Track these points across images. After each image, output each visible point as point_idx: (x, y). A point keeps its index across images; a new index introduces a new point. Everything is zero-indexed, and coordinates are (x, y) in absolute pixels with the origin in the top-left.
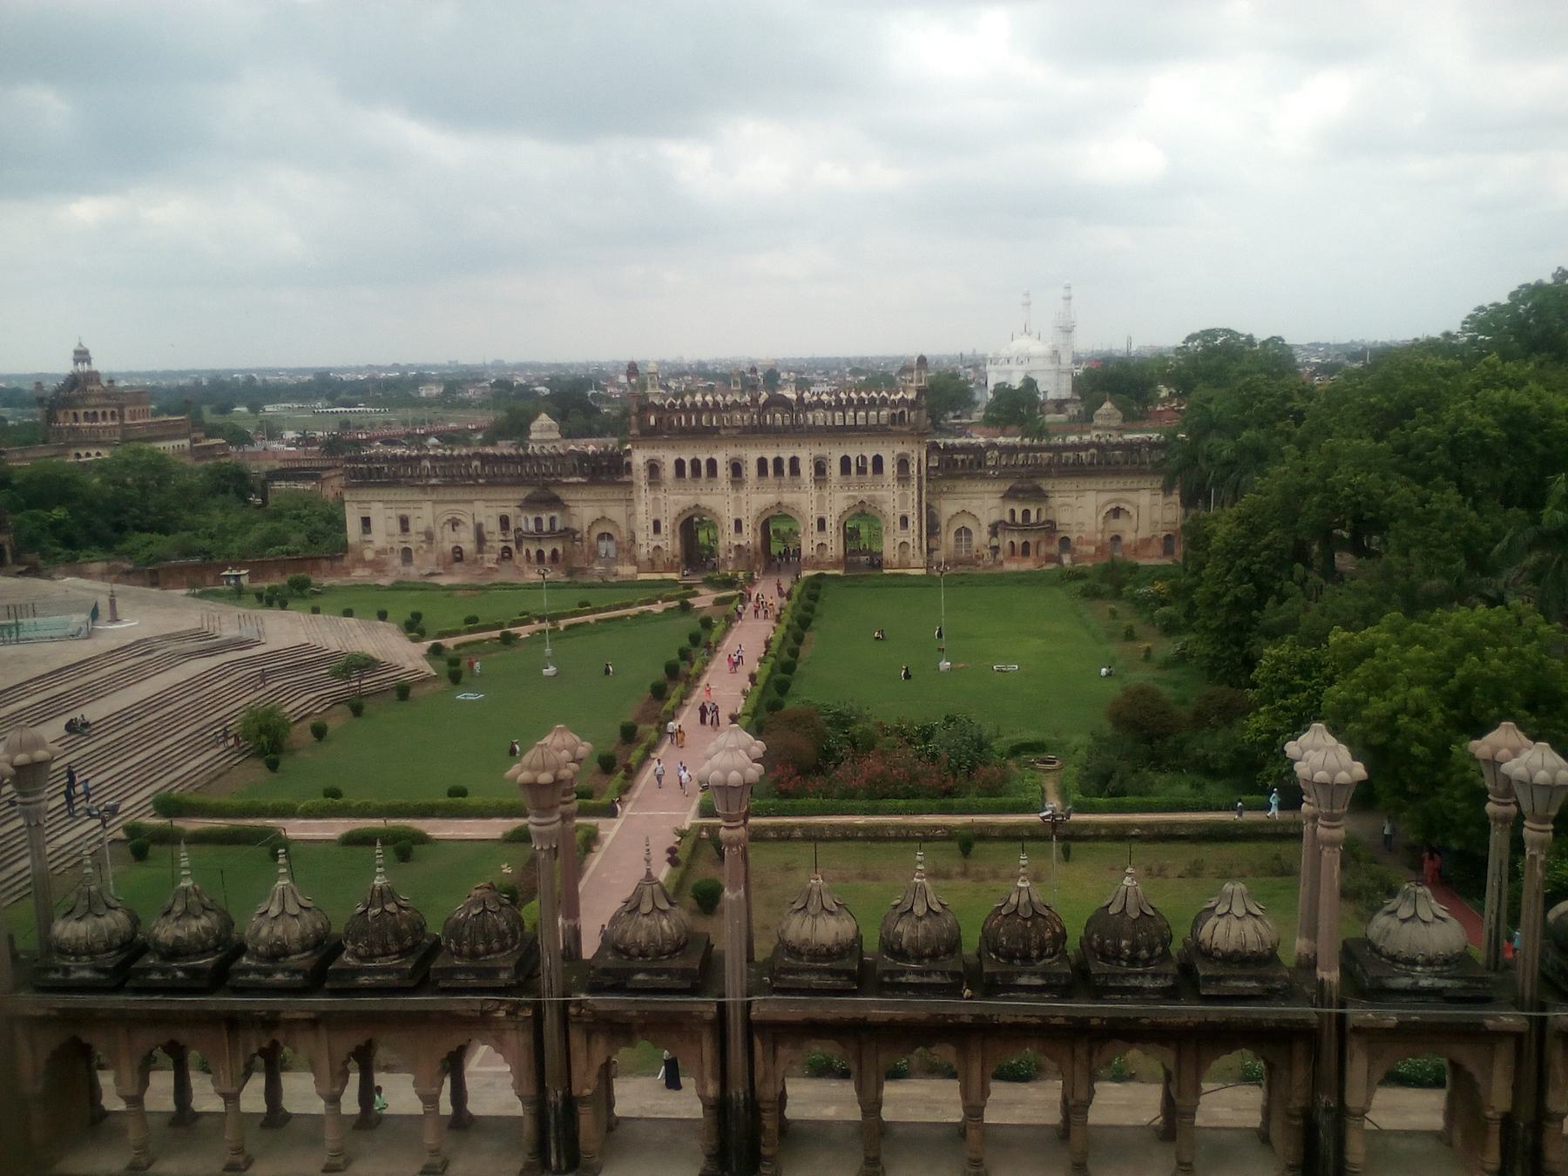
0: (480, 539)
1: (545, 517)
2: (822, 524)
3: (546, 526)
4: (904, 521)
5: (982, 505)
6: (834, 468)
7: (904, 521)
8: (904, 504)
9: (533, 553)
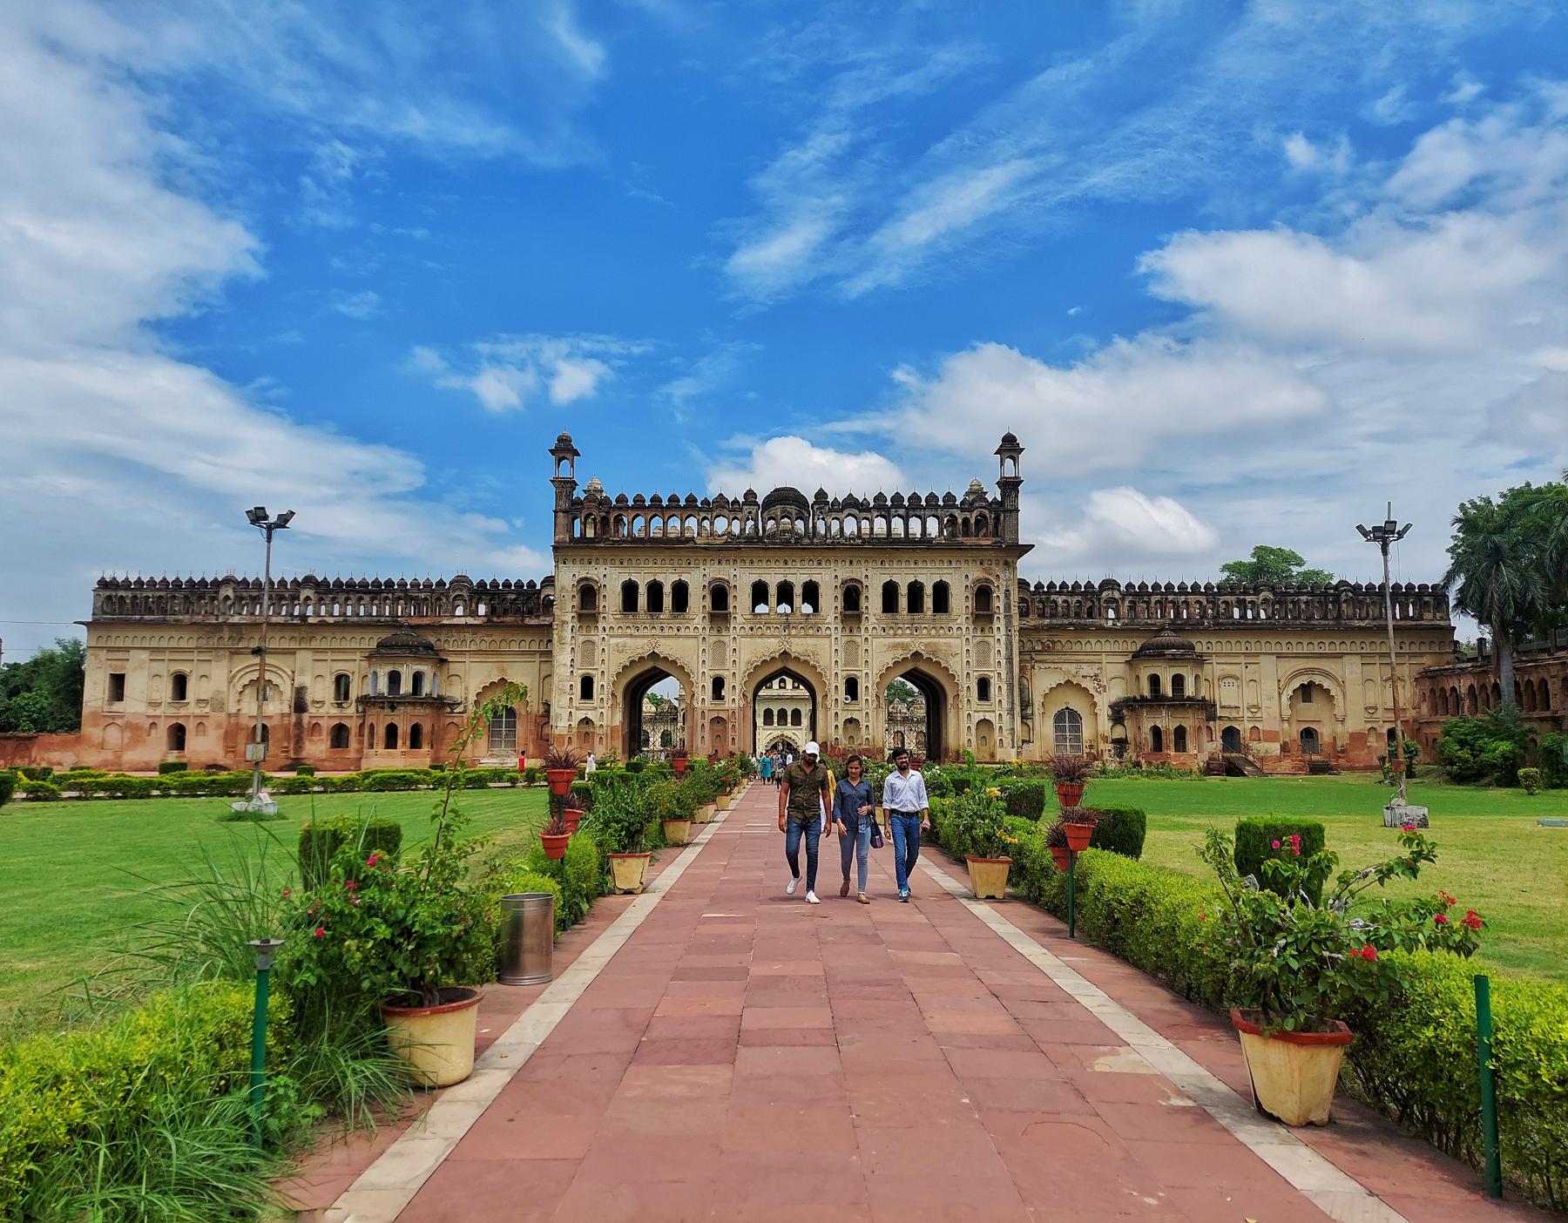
1: (407, 672)
2: (852, 686)
3: (406, 687)
4: (984, 686)
5: (1105, 672)
6: (872, 601)
7: (984, 686)
8: (983, 660)
9: (381, 731)
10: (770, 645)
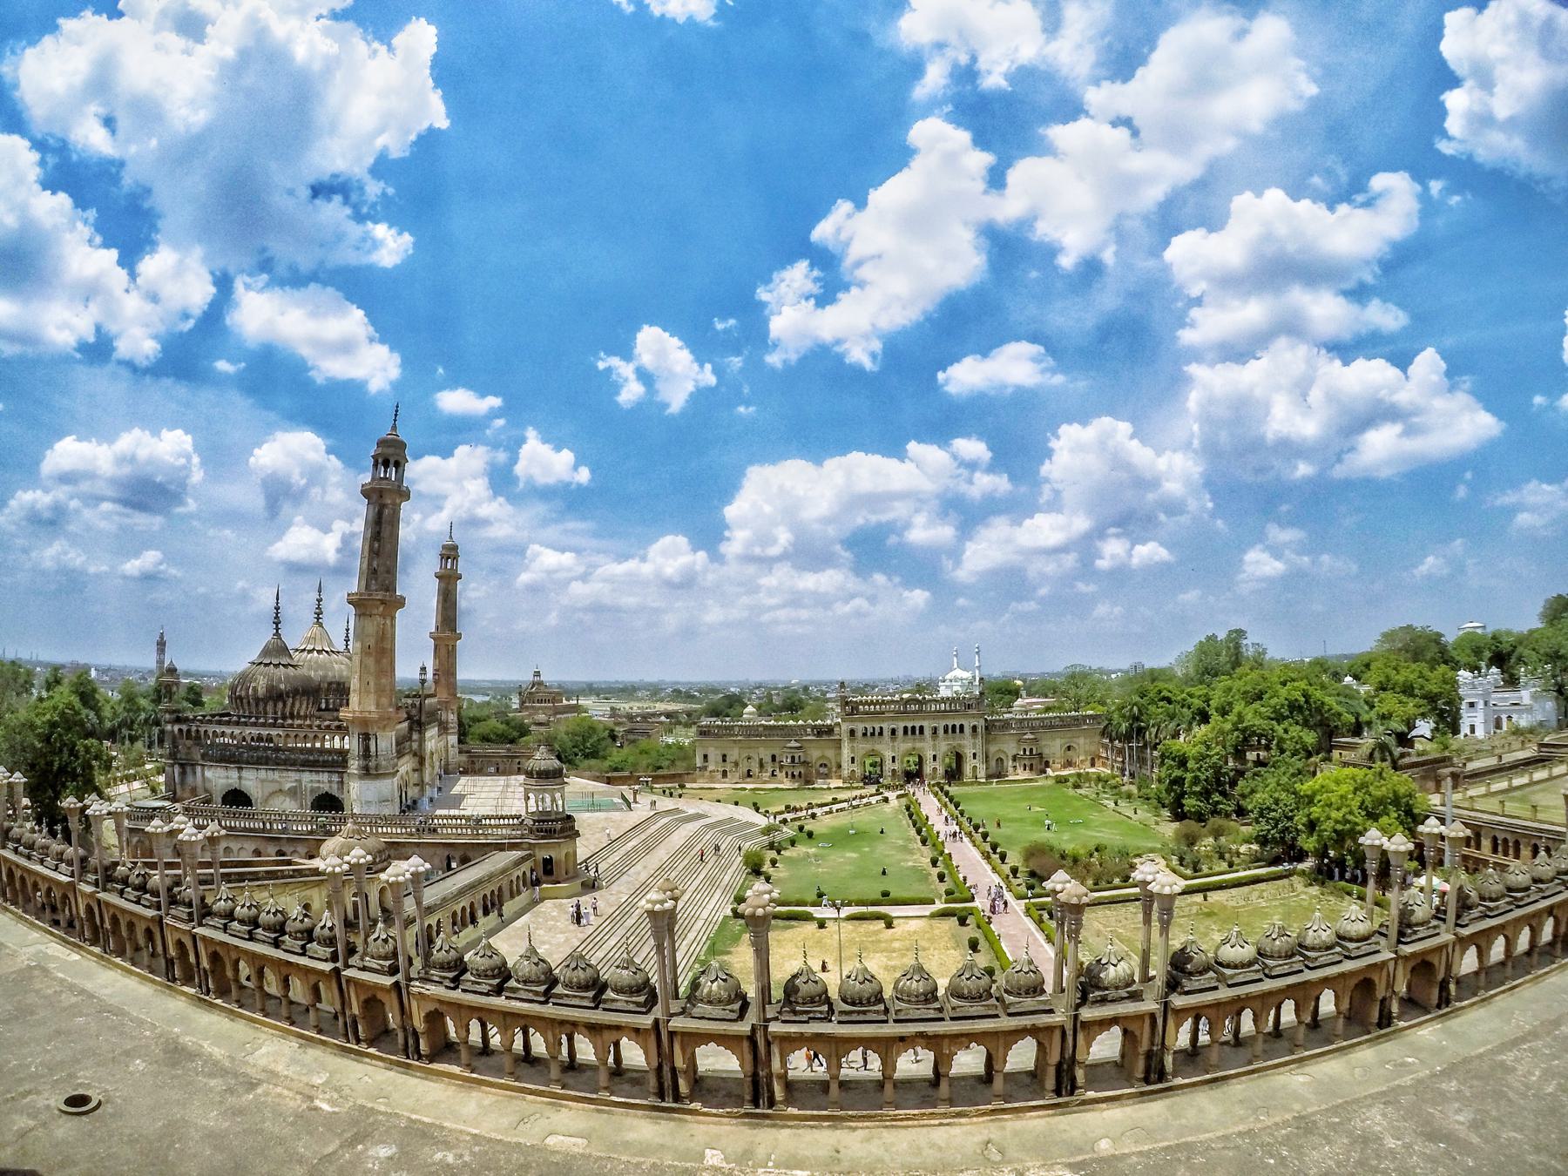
0: (761, 765)
6: (941, 731)
10: (910, 745)
